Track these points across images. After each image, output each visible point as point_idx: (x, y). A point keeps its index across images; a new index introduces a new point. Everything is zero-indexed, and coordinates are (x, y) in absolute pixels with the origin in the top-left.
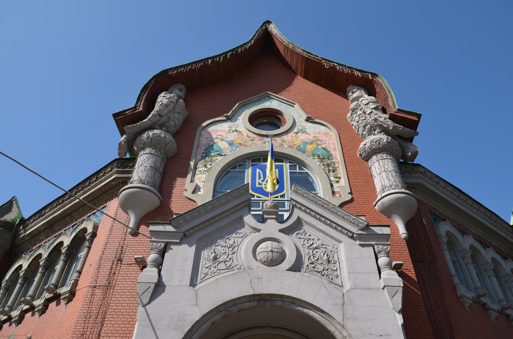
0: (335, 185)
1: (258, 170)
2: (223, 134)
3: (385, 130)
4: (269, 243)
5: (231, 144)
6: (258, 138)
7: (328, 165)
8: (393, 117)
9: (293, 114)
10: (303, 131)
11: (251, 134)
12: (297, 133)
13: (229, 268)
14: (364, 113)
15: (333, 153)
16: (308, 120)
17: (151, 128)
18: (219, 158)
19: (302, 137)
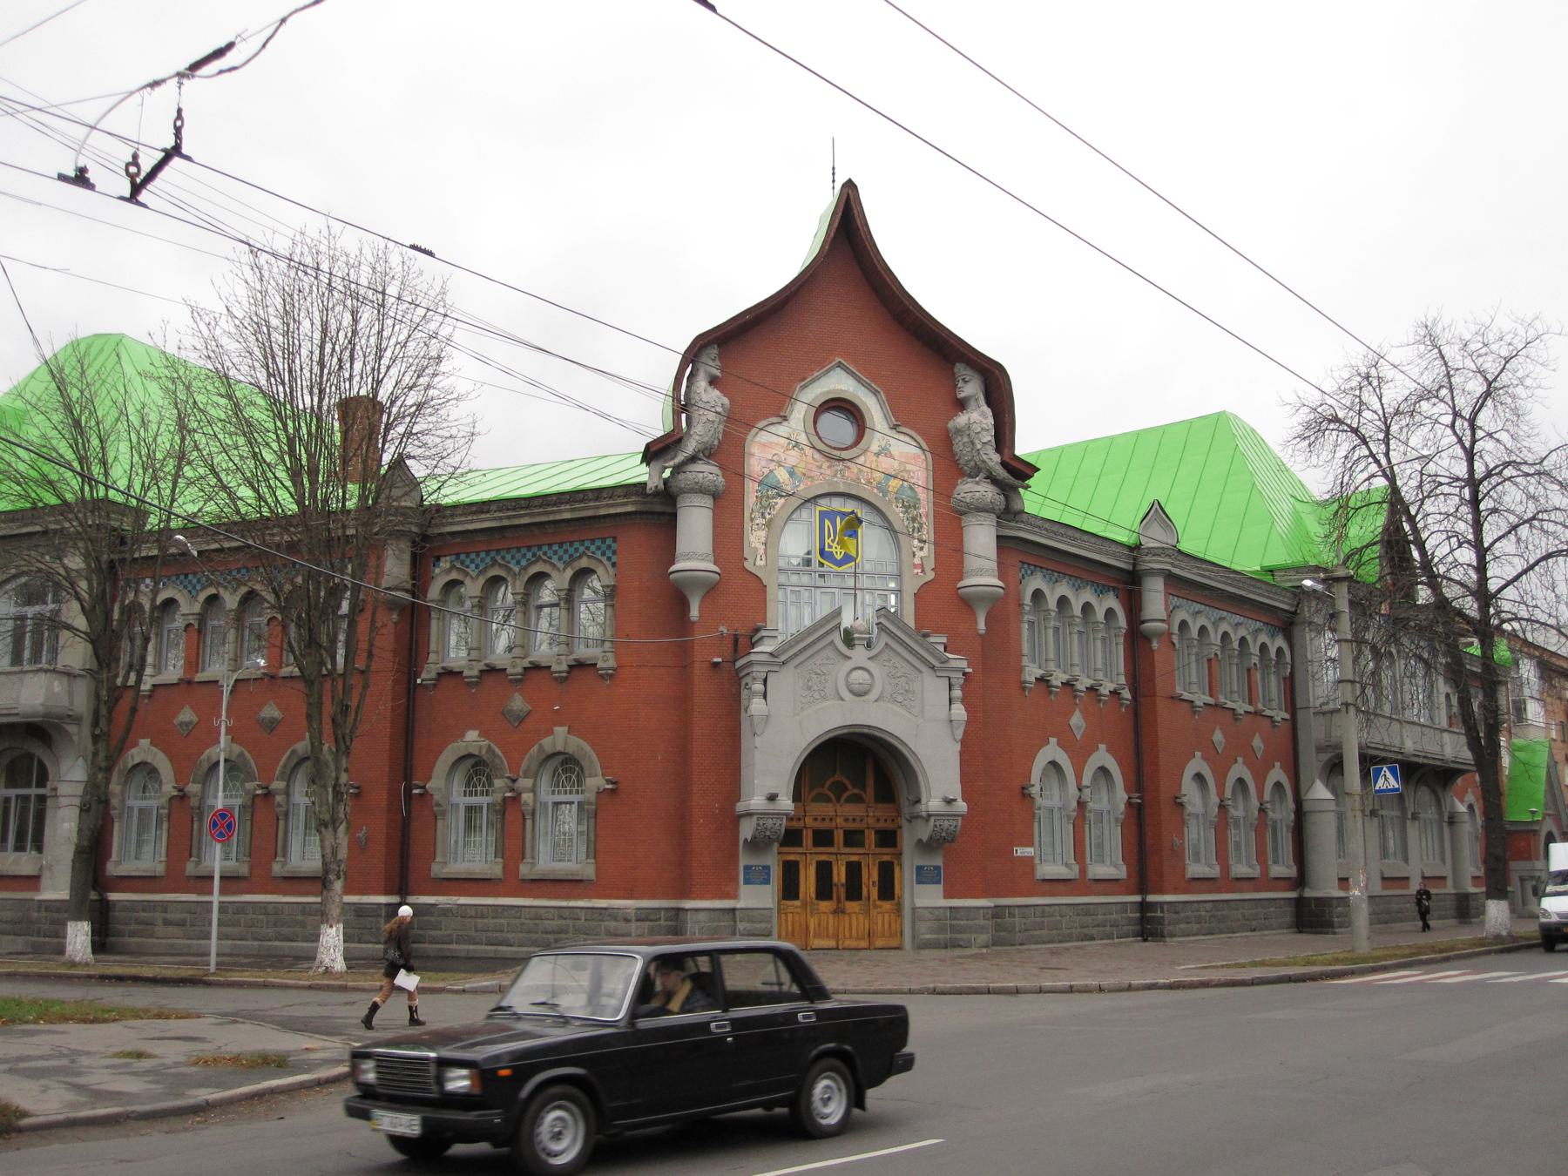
0: (920, 554)
1: (827, 522)
2: (780, 451)
3: (994, 481)
4: (860, 672)
5: (792, 474)
6: (826, 465)
7: (914, 520)
8: (1004, 464)
9: (872, 407)
10: (884, 452)
11: (817, 456)
12: (878, 455)
13: (825, 698)
14: (973, 443)
15: (922, 495)
16: (894, 427)
17: (693, 459)
18: (781, 501)
19: (886, 464)
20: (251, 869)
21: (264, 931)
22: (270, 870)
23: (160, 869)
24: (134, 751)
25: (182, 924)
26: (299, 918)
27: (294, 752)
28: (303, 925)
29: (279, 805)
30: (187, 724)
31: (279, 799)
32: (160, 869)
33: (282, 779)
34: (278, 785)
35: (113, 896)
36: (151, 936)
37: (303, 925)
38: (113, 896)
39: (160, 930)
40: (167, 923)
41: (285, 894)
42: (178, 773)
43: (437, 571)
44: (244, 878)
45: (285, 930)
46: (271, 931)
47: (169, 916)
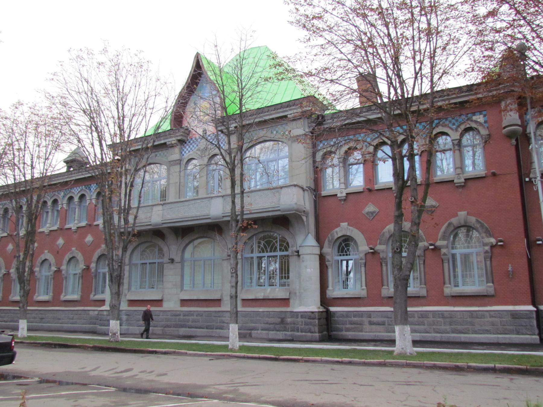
20: (427, 292)
21: (443, 327)
22: (443, 291)
23: (363, 293)
24: (337, 229)
25: (383, 324)
26: (469, 319)
27: (450, 224)
28: (472, 324)
29: (445, 254)
30: (372, 213)
31: (443, 251)
32: (363, 293)
33: (444, 238)
34: (439, 243)
35: (332, 309)
36: (361, 331)
37: (472, 324)
38: (332, 309)
39: (367, 327)
40: (371, 323)
41: (454, 305)
42: (369, 240)
43: (528, 117)
44: (424, 297)
45: (459, 327)
46: (448, 328)
47: (372, 319)
